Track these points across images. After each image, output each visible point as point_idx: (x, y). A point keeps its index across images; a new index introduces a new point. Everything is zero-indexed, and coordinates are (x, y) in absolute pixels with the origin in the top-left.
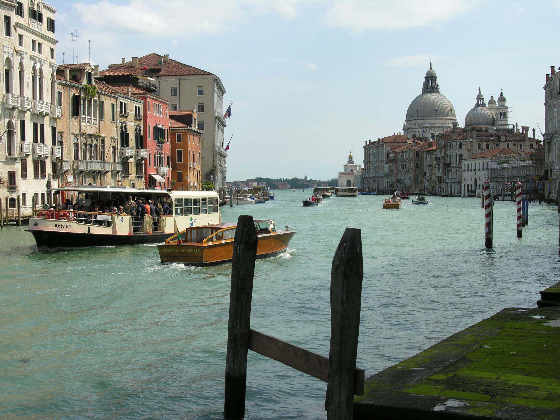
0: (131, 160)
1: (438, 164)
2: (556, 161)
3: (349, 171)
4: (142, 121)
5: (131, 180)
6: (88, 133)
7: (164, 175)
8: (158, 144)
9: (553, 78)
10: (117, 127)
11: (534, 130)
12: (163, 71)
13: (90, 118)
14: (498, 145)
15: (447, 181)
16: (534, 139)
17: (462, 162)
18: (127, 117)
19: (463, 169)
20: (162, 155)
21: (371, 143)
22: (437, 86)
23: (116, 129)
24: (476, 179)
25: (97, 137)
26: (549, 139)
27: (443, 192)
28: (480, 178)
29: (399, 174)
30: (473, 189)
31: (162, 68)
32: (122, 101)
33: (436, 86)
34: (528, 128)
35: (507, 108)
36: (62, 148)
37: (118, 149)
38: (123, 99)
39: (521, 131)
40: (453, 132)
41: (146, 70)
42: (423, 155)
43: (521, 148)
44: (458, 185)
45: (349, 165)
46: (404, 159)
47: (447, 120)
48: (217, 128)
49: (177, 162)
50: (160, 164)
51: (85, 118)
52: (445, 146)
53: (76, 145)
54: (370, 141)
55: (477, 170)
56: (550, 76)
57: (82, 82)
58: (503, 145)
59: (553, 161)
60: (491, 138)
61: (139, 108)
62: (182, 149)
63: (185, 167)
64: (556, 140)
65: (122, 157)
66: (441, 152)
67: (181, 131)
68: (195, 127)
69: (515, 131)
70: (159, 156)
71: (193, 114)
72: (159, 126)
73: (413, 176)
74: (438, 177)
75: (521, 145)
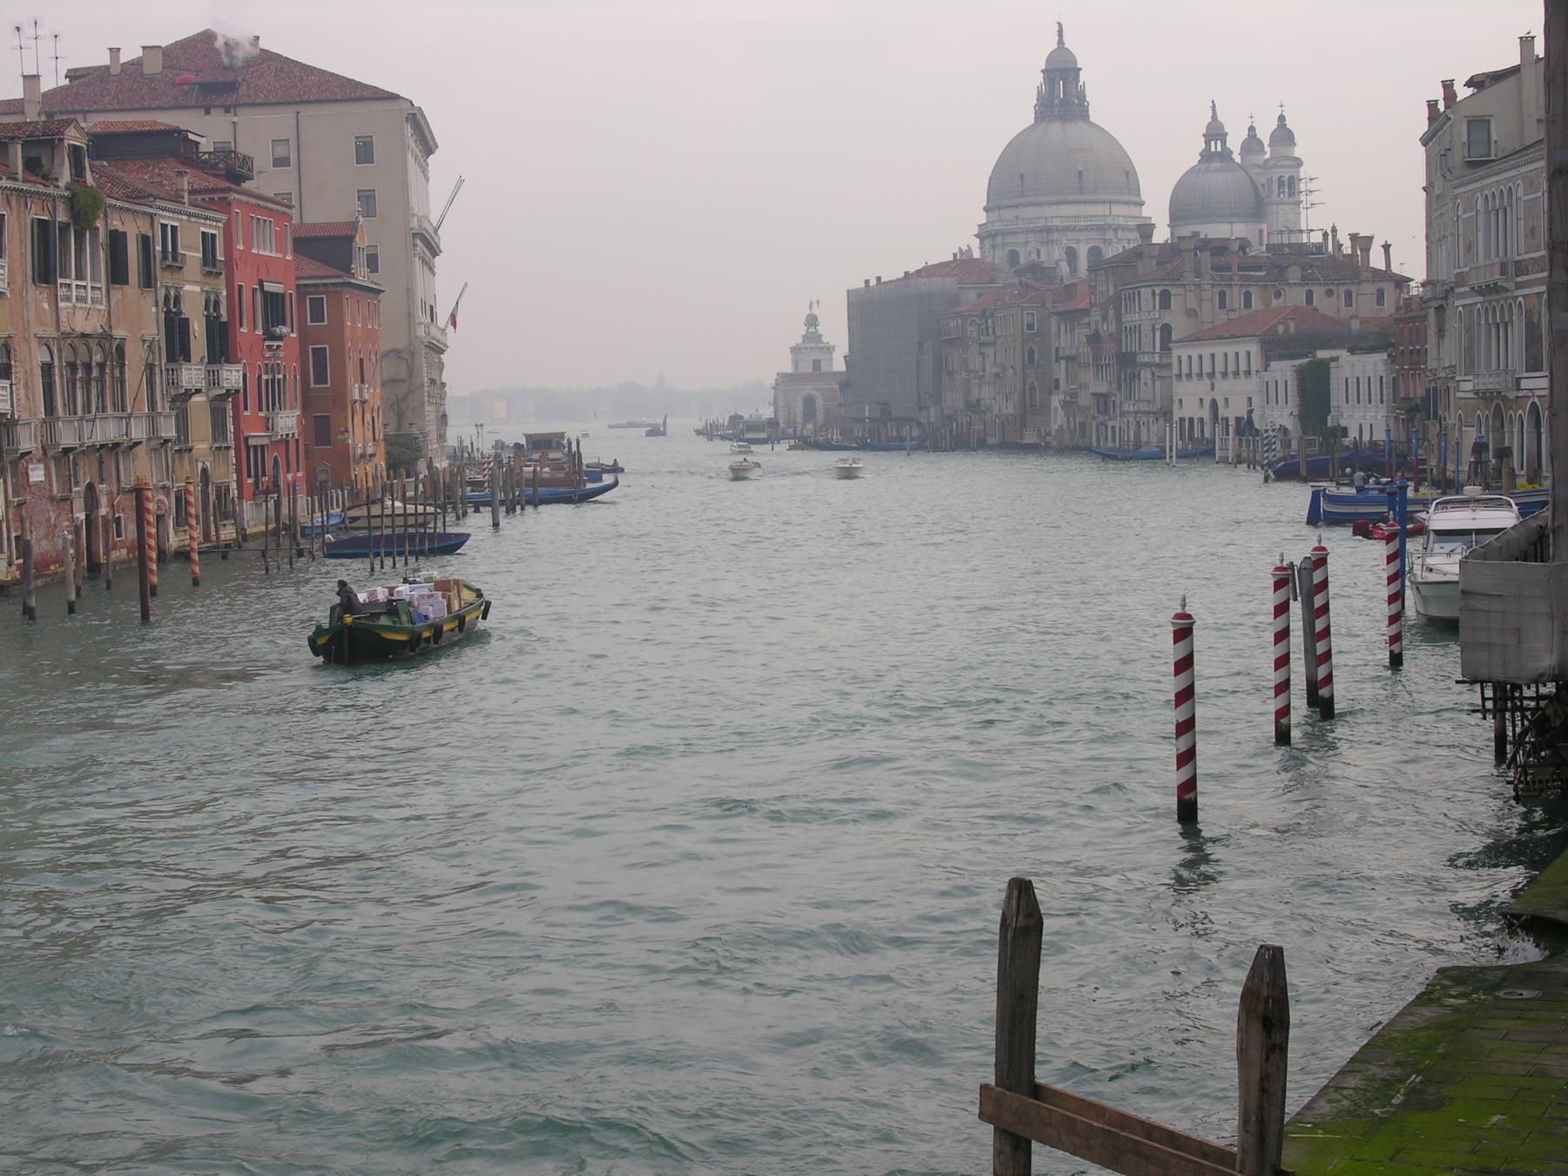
0: (196, 399)
1: (1096, 357)
2: (1460, 364)
3: (807, 368)
4: (223, 276)
5: (197, 461)
6: (79, 329)
7: (287, 435)
8: (267, 343)
10: (157, 306)
11: (1386, 247)
12: (243, 90)
13: (84, 283)
14: (1278, 295)
15: (1126, 407)
16: (1386, 275)
17: (1170, 349)
18: (181, 268)
19: (1175, 371)
20: (279, 373)
22: (1082, 97)
23: (154, 309)
24: (1214, 403)
25: (106, 336)
26: (1442, 298)
28: (1226, 400)
31: (239, 79)
32: (165, 222)
33: (1077, 97)
34: (1370, 239)
35: (1298, 163)
36: (11, 385)
37: (161, 371)
38: (168, 214)
41: (186, 87)
43: (1349, 303)
44: (1157, 420)
45: (806, 348)
46: (991, 339)
47: (1113, 206)
48: (418, 263)
49: (312, 385)
50: (274, 405)
51: (69, 285)
52: (1117, 301)
53: (47, 369)
54: (879, 279)
55: (1218, 376)
56: (1441, 107)
57: (57, 179)
59: (1455, 366)
60: (1258, 274)
61: (213, 236)
62: (327, 346)
63: (339, 398)
65: (173, 393)
66: (1105, 318)
67: (322, 289)
68: (361, 276)
69: (1330, 249)
70: (270, 377)
71: (354, 233)
72: (269, 287)
74: (1097, 396)
75: (1349, 294)
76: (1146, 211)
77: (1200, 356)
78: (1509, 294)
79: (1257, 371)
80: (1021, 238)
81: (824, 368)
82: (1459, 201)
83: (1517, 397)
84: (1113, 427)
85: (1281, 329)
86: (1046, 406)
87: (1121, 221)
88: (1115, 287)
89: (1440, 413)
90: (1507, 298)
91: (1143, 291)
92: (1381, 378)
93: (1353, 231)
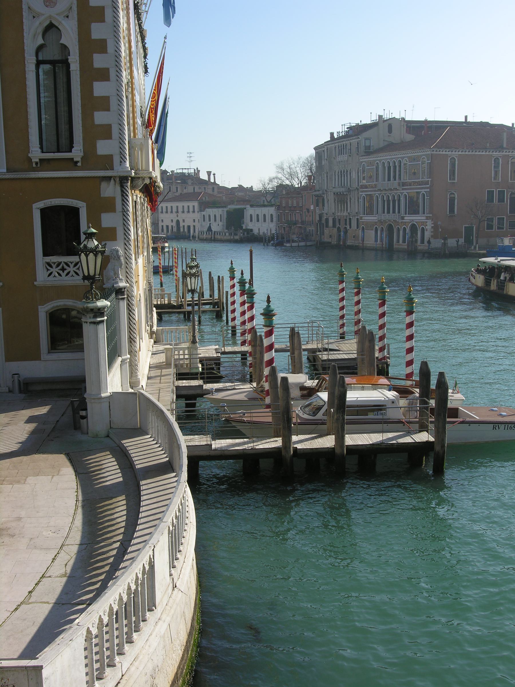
9: (360, 137)
11: (214, 174)
14: (185, 189)
19: (160, 210)
24: (178, 222)
28: (184, 221)
30: (175, 230)
34: (211, 172)
64: (363, 193)
75: (205, 188)
77: (172, 207)
78: (398, 191)
79: (198, 212)
82: (364, 163)
83: (402, 222)
85: (204, 198)
89: (338, 225)
90: (397, 193)
92: (272, 215)
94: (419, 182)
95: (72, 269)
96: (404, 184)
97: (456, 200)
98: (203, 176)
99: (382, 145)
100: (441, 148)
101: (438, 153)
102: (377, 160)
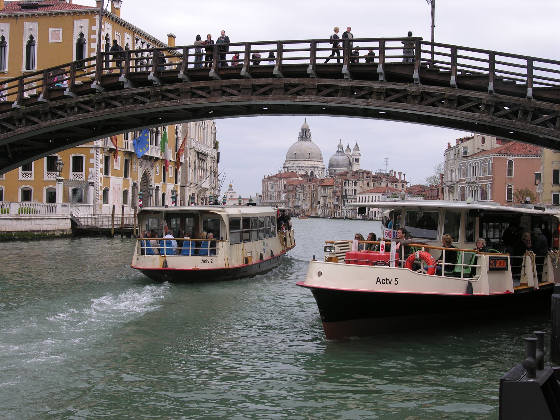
11: (404, 175)
14: (380, 184)
15: (343, 208)
16: (404, 181)
19: (358, 200)
21: (269, 177)
27: (339, 215)
29: (297, 201)
34: (401, 173)
35: (360, 155)
39: (393, 175)
40: (348, 173)
42: (318, 189)
52: (342, 183)
54: (268, 175)
56: (454, 143)
58: (384, 185)
64: (460, 186)
73: (310, 203)
75: (396, 185)
76: (324, 164)
80: (294, 168)
81: (233, 197)
84: (339, 213)
85: (387, 191)
86: (316, 207)
87: (319, 166)
88: (341, 180)
91: (350, 181)
93: (395, 171)
94: (487, 177)
95: (80, 176)
96: (480, 179)
97: (513, 191)
98: (397, 177)
99: (476, 151)
100: (501, 154)
101: (499, 157)
102: (467, 162)
